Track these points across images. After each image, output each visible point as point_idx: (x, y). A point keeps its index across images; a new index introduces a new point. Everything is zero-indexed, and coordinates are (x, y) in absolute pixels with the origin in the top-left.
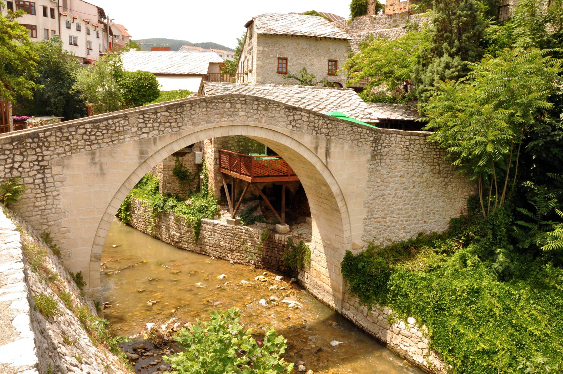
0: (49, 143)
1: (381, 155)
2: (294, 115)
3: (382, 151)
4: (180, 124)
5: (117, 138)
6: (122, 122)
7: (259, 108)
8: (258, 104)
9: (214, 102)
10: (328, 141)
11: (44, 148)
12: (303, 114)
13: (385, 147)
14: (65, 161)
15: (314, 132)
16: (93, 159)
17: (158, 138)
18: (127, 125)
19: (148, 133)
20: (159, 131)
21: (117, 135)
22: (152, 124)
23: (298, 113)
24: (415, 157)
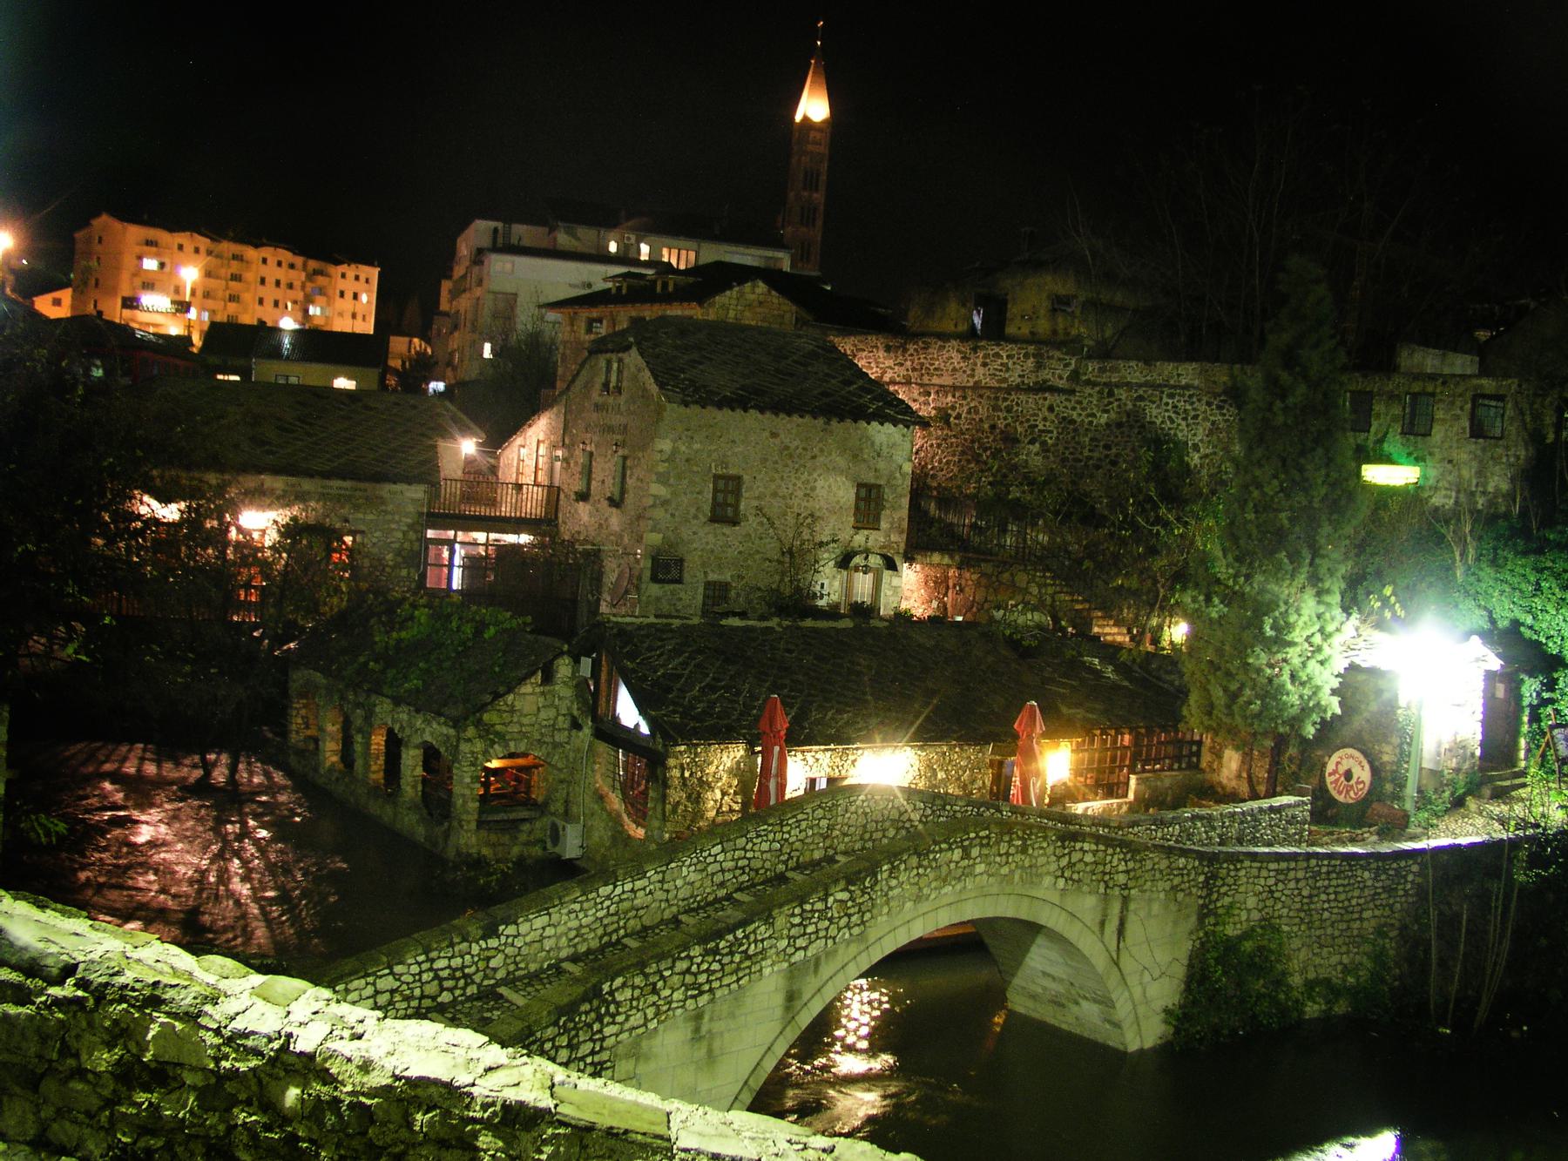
0: (618, 1004)
1: (1216, 915)
2: (1070, 854)
3: (1219, 904)
4: (867, 917)
5: (747, 971)
6: (763, 928)
7: (1012, 850)
8: (1011, 840)
9: (933, 851)
10: (1126, 900)
11: (607, 1019)
12: (1086, 846)
13: (1225, 894)
14: (644, 1044)
15: (1102, 885)
16: (697, 1030)
17: (823, 958)
18: (770, 937)
19: (805, 949)
20: (826, 937)
21: (748, 963)
22: (816, 924)
23: (1078, 845)
24: (1285, 911)
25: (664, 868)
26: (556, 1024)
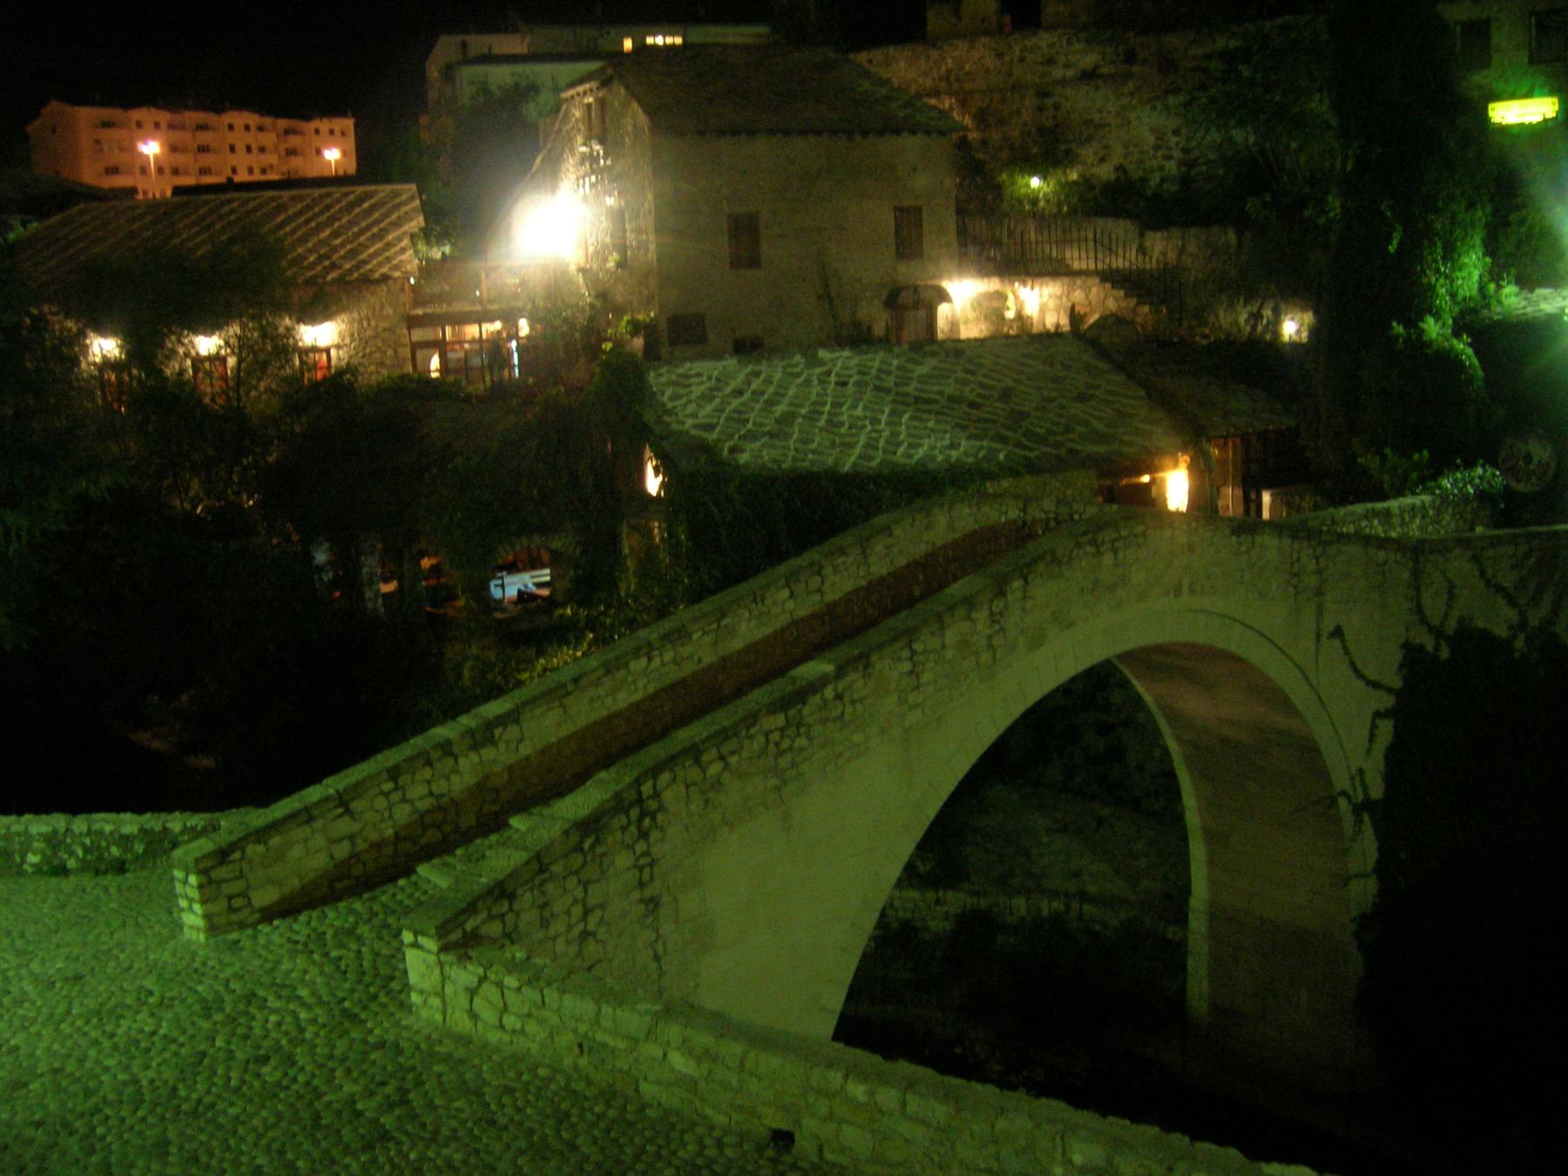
25: (715, 626)
26: (578, 848)
